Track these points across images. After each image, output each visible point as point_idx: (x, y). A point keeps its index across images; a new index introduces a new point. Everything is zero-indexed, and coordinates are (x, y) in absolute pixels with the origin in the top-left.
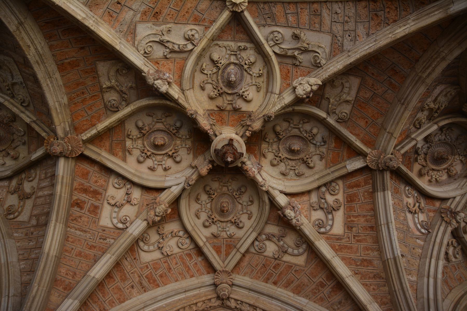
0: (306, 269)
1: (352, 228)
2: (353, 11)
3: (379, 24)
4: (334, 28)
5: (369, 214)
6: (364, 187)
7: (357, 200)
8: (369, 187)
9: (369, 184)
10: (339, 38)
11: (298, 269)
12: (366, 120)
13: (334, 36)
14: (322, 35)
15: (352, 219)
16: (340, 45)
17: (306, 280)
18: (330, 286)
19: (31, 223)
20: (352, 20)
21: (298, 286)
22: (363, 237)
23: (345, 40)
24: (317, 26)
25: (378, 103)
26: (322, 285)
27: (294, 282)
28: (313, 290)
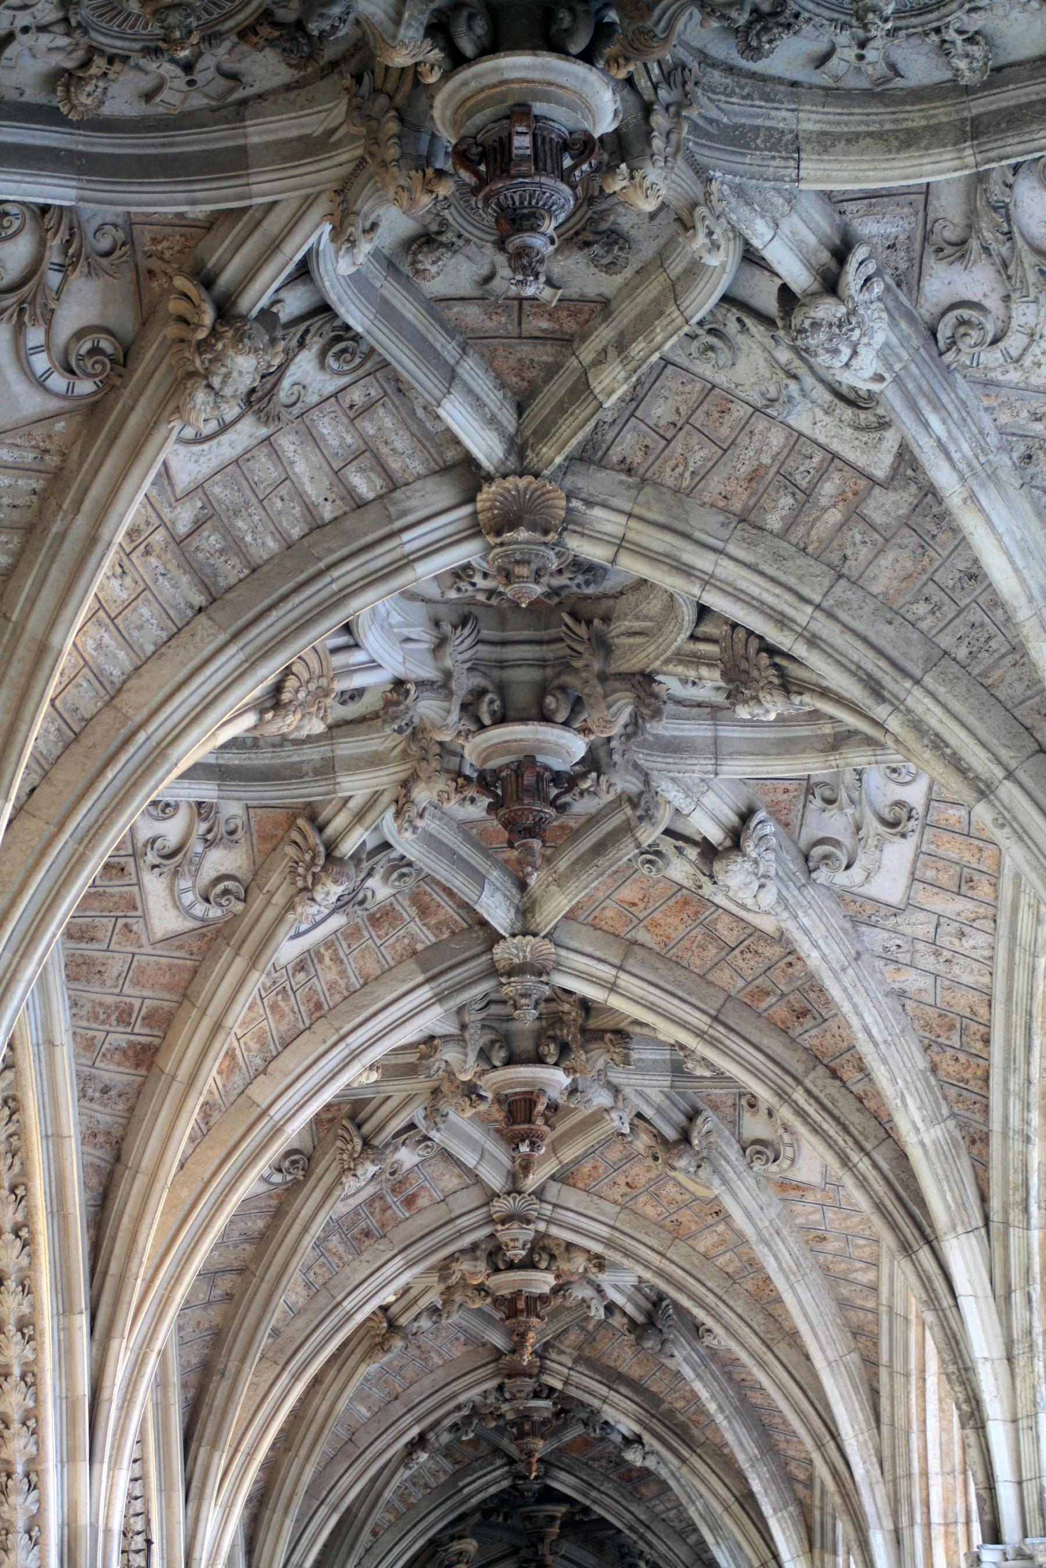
0: (148, 949)
1: (303, 969)
2: (966, 979)
3: (928, 1026)
4: (921, 916)
5: (353, 979)
6: (424, 929)
7: (382, 932)
8: (426, 937)
9: (436, 936)
10: (892, 920)
11: (135, 928)
12: (641, 905)
13: (897, 911)
14: (903, 881)
15: (327, 955)
16: (874, 918)
17: (116, 966)
18: (132, 1038)
19: (178, 510)
20: (942, 968)
21: (88, 962)
22: (287, 1010)
23: (886, 935)
24: (930, 874)
25: (703, 947)
26: (124, 1016)
27: (95, 945)
28: (101, 1004)
